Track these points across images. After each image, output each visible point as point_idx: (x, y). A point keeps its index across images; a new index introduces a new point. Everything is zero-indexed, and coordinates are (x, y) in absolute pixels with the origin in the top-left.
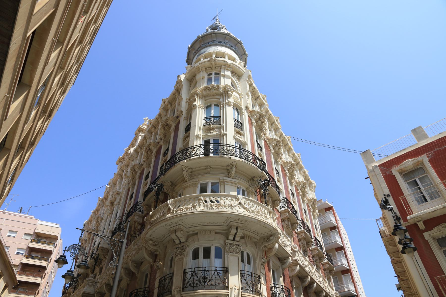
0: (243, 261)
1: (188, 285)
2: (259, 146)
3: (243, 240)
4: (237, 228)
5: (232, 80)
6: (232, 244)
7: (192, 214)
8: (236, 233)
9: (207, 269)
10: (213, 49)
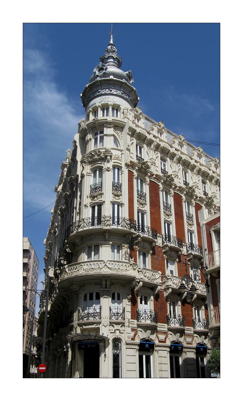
2: (141, 196)
3: (112, 287)
4: (106, 281)
5: (113, 135)
6: (104, 291)
7: (77, 277)
8: (106, 283)
10: (97, 102)
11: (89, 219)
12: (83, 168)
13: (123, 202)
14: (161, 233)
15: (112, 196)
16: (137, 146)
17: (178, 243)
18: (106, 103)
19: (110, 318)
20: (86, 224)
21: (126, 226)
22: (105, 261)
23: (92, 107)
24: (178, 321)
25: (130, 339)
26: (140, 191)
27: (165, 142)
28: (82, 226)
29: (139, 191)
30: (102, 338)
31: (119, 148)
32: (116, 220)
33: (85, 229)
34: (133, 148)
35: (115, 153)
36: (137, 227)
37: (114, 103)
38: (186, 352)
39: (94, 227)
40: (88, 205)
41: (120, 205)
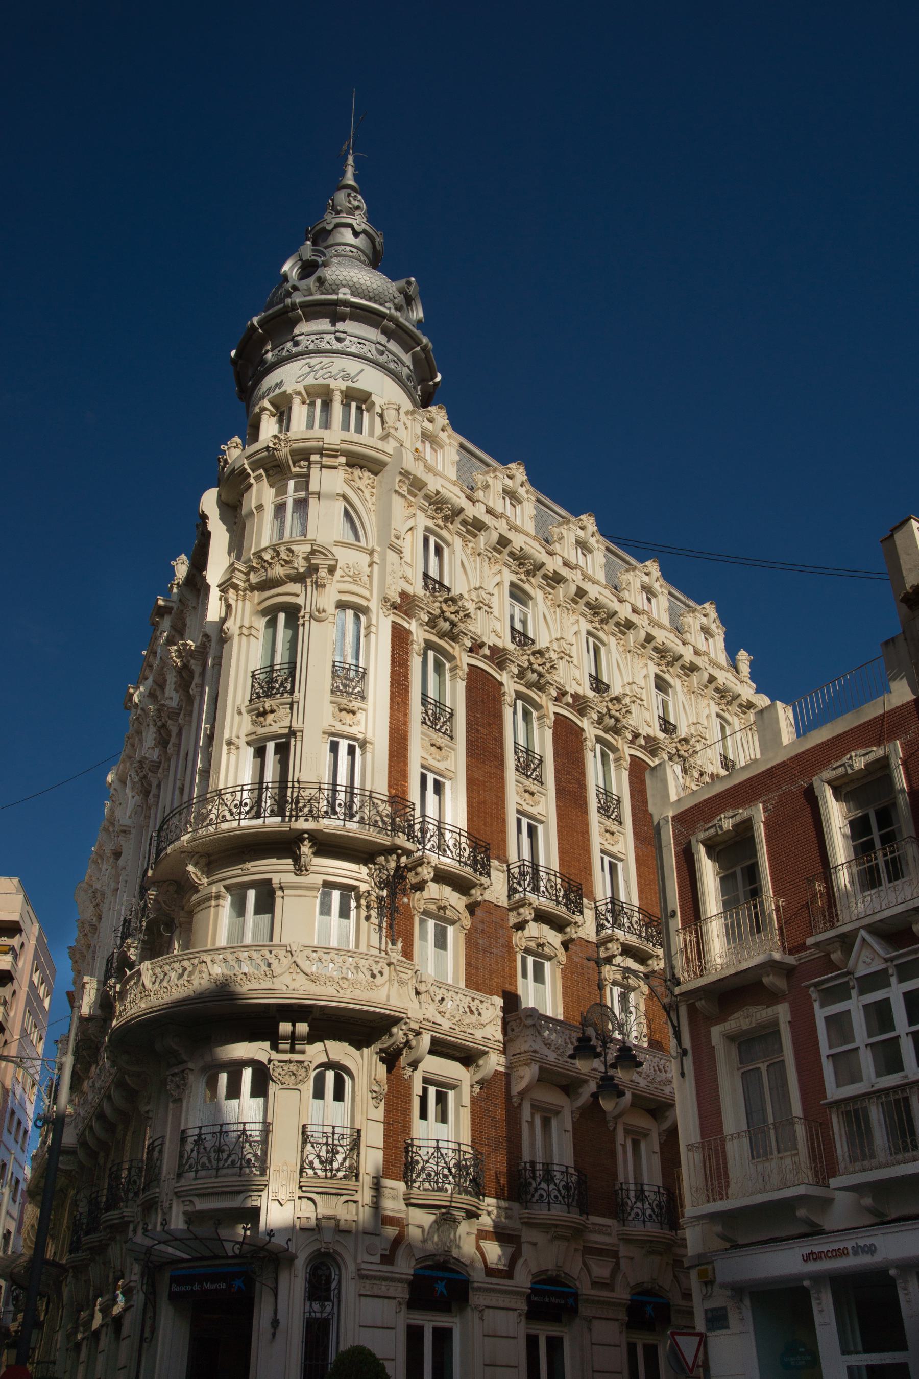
0: (319, 1093)
1: (187, 1167)
11: (242, 790)
12: (229, 607)
13: (369, 736)
14: (503, 859)
15: (329, 709)
16: (426, 540)
17: (566, 896)
18: (321, 381)
19: (301, 1171)
20: (230, 811)
21: (376, 821)
22: (294, 949)
23: (272, 395)
24: (563, 1192)
25: (377, 1259)
26: (433, 702)
27: (527, 534)
28: (213, 816)
29: (429, 700)
30: (267, 1250)
31: (363, 543)
32: (341, 796)
33: (225, 826)
34: (412, 546)
35: (345, 557)
36: (417, 827)
37: (349, 383)
38: (590, 1321)
39: (259, 822)
40: (242, 742)
41: (357, 746)
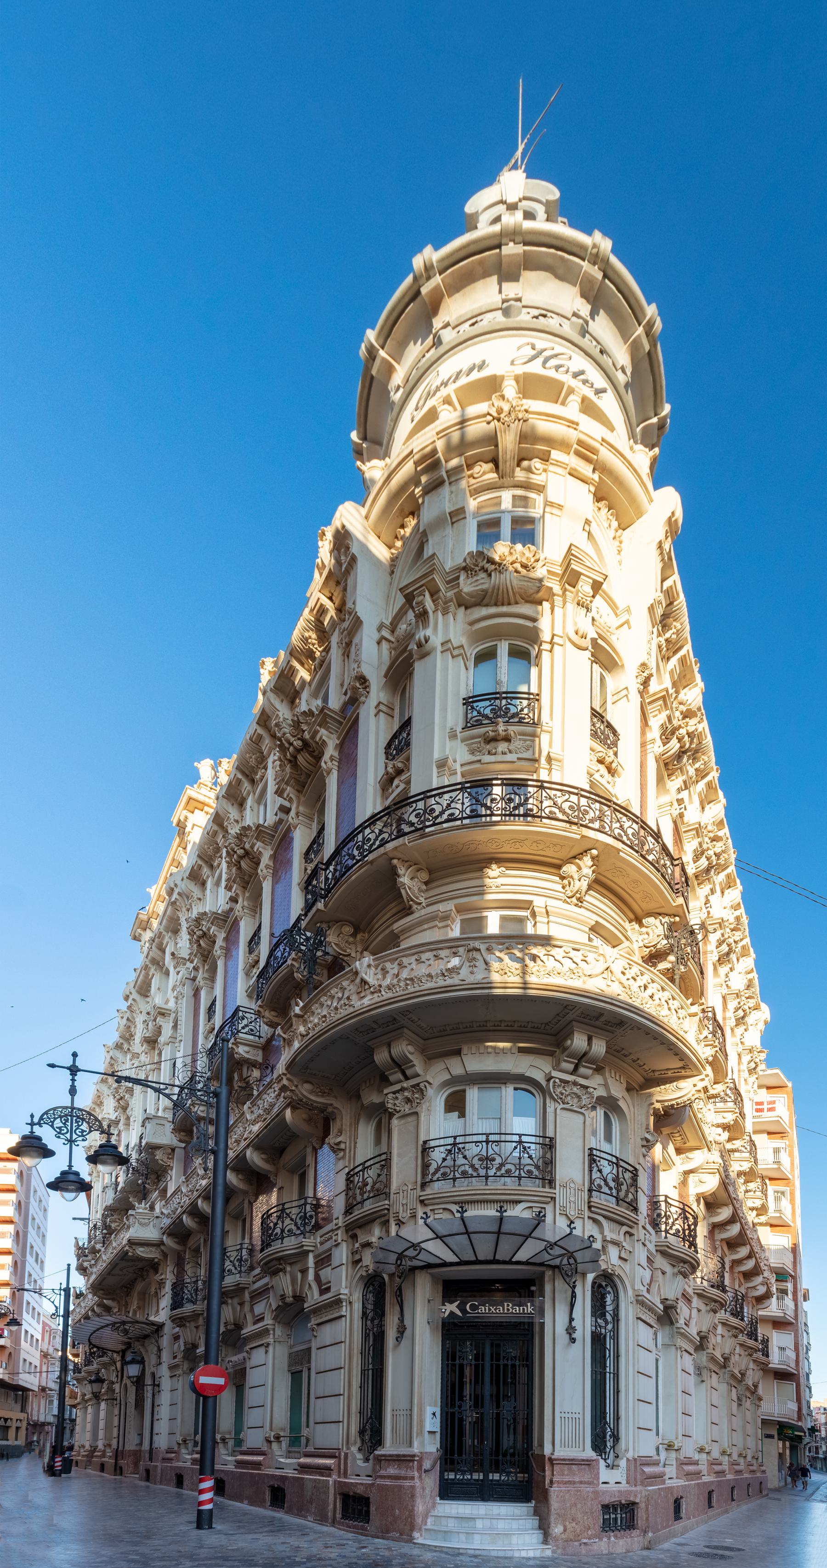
1: (438, 1175)
9: (492, 1138)
